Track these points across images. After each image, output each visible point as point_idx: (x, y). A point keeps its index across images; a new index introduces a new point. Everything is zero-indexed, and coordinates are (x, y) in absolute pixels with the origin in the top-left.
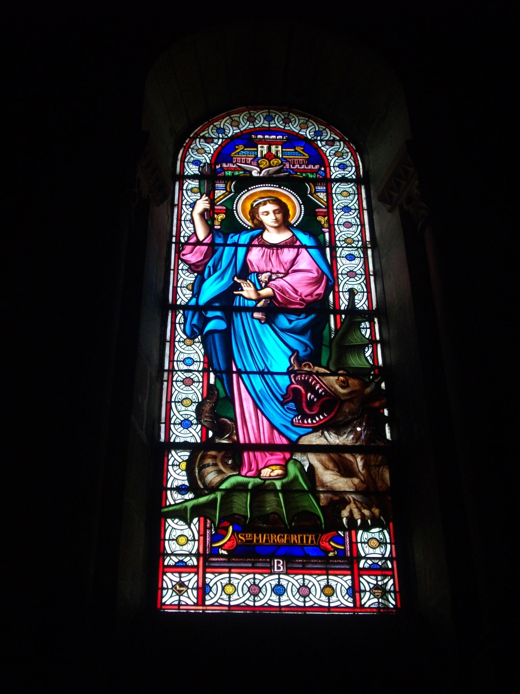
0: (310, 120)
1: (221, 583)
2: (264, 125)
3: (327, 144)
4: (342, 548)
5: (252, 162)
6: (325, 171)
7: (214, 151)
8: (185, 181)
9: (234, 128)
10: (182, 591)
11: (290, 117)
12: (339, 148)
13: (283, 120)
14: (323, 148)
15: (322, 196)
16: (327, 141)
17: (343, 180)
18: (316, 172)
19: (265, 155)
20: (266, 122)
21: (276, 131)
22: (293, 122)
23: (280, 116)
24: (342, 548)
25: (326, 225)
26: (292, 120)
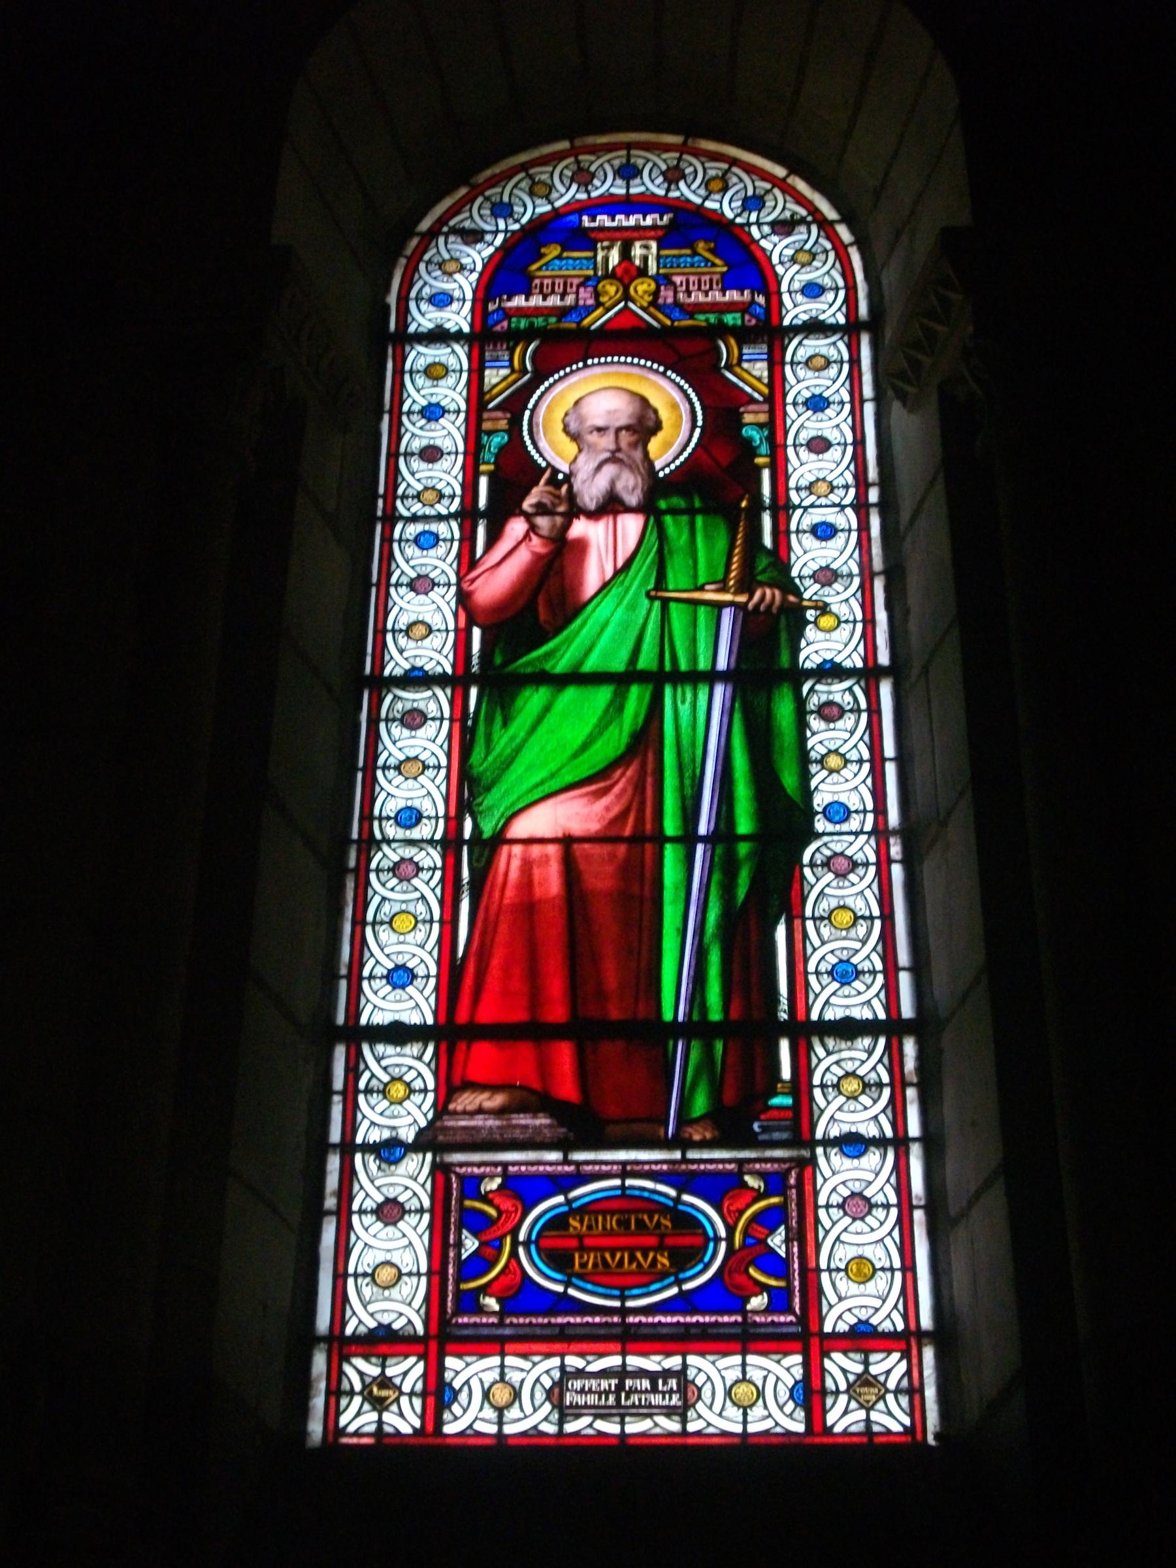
2: (614, 190)
4: (782, 1284)
5: (582, 290)
6: (768, 309)
8: (408, 348)
9: (538, 201)
10: (386, 1398)
11: (683, 165)
12: (806, 241)
13: (663, 173)
14: (763, 243)
15: (760, 369)
16: (773, 224)
17: (815, 327)
18: (744, 308)
19: (614, 268)
20: (619, 182)
21: (645, 204)
23: (655, 164)
25: (764, 449)
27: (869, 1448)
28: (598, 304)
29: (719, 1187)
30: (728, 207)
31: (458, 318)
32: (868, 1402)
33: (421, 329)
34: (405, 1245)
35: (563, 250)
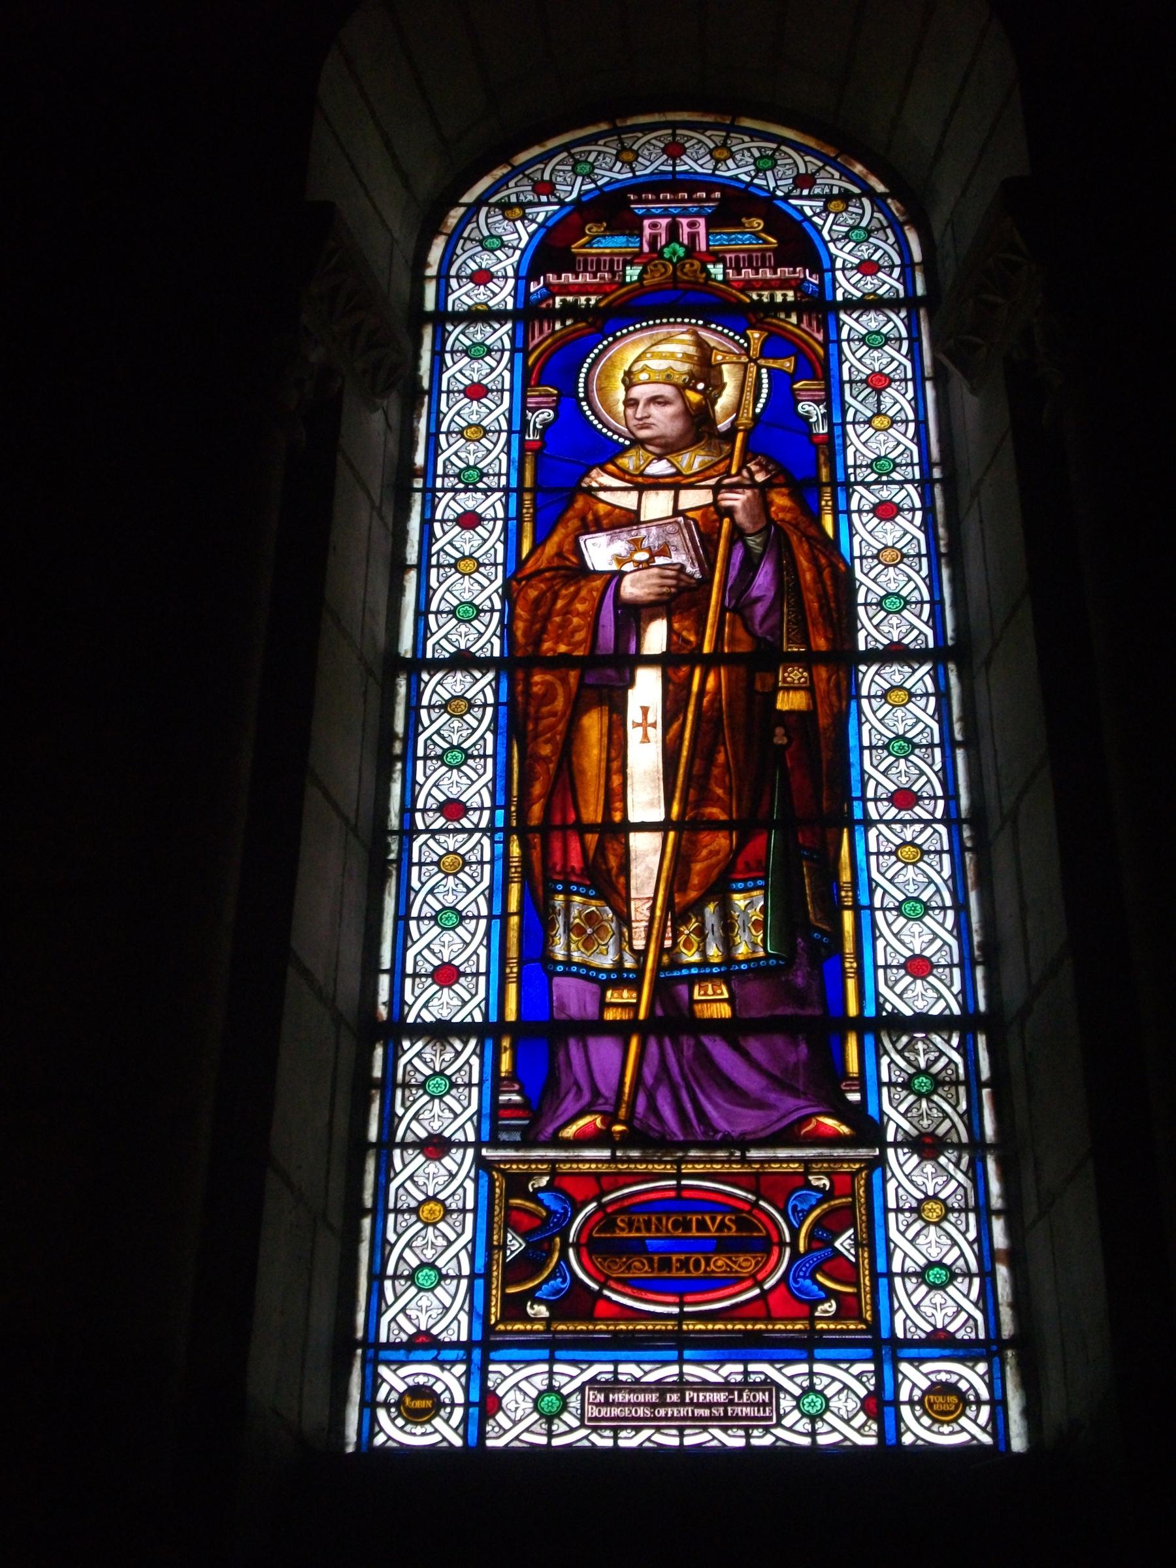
21: (691, 183)
30: (776, 182)
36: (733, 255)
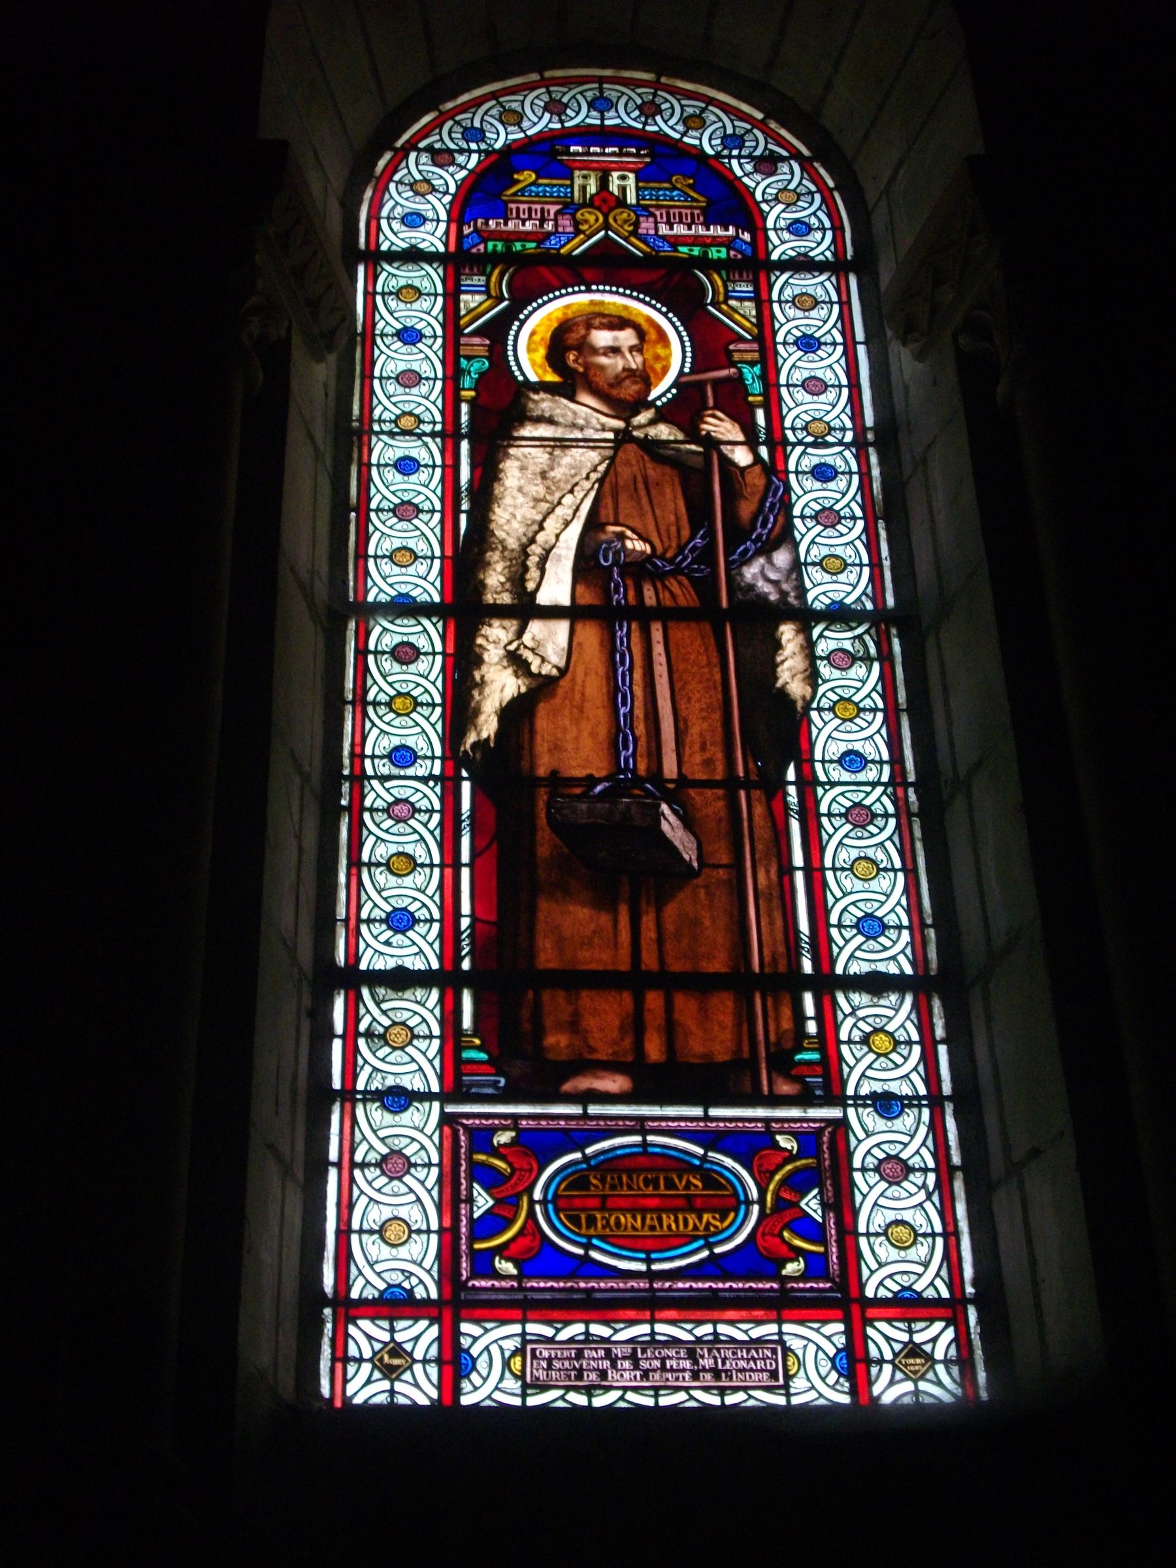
0: (711, 108)
1: (501, 1348)
3: (756, 170)
5: (560, 218)
6: (753, 243)
7: (458, 187)
12: (790, 181)
13: (638, 107)
14: (746, 180)
15: (749, 308)
17: (802, 264)
18: (729, 243)
19: (592, 196)
20: (594, 113)
21: (621, 137)
22: (667, 115)
23: (630, 98)
24: (821, 1249)
25: (756, 387)
26: (664, 107)
27: (917, 1426)
28: (578, 232)
29: (751, 1146)
31: (432, 238)
32: (915, 1372)
33: (394, 248)
34: (415, 1201)
35: (538, 177)
36: (677, 211)
